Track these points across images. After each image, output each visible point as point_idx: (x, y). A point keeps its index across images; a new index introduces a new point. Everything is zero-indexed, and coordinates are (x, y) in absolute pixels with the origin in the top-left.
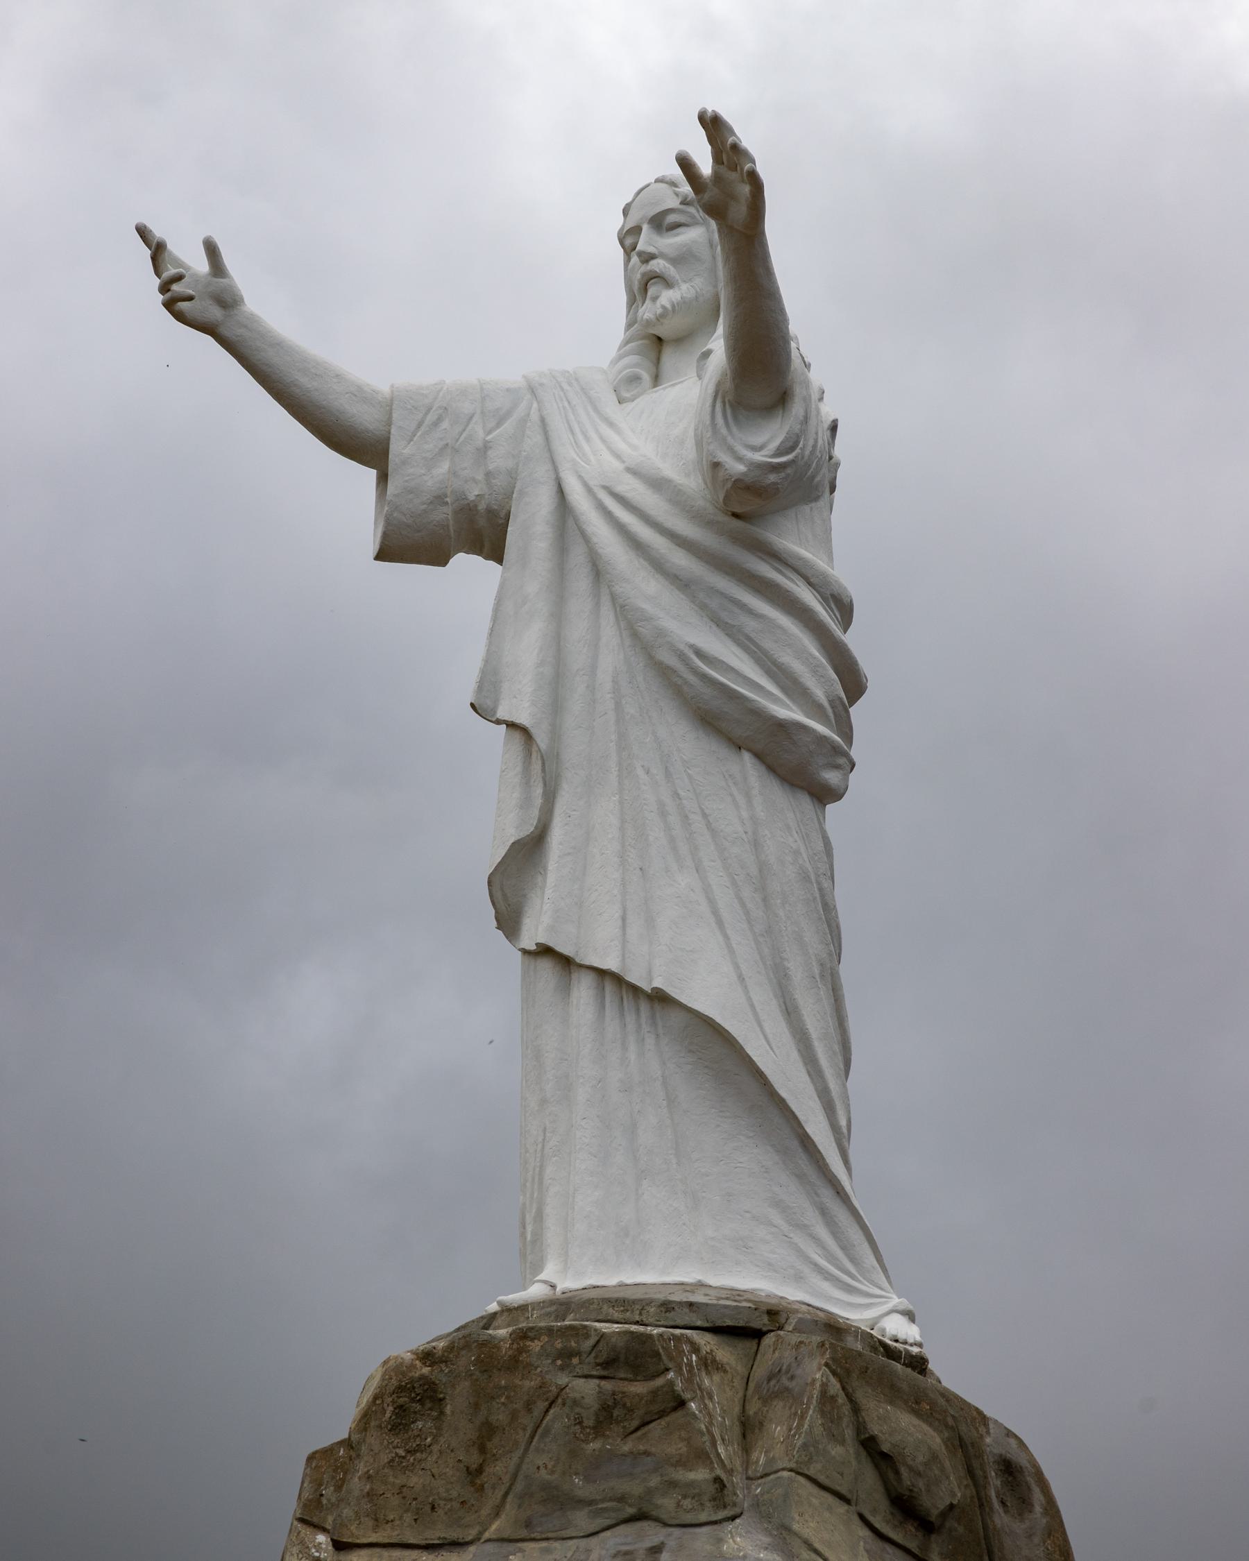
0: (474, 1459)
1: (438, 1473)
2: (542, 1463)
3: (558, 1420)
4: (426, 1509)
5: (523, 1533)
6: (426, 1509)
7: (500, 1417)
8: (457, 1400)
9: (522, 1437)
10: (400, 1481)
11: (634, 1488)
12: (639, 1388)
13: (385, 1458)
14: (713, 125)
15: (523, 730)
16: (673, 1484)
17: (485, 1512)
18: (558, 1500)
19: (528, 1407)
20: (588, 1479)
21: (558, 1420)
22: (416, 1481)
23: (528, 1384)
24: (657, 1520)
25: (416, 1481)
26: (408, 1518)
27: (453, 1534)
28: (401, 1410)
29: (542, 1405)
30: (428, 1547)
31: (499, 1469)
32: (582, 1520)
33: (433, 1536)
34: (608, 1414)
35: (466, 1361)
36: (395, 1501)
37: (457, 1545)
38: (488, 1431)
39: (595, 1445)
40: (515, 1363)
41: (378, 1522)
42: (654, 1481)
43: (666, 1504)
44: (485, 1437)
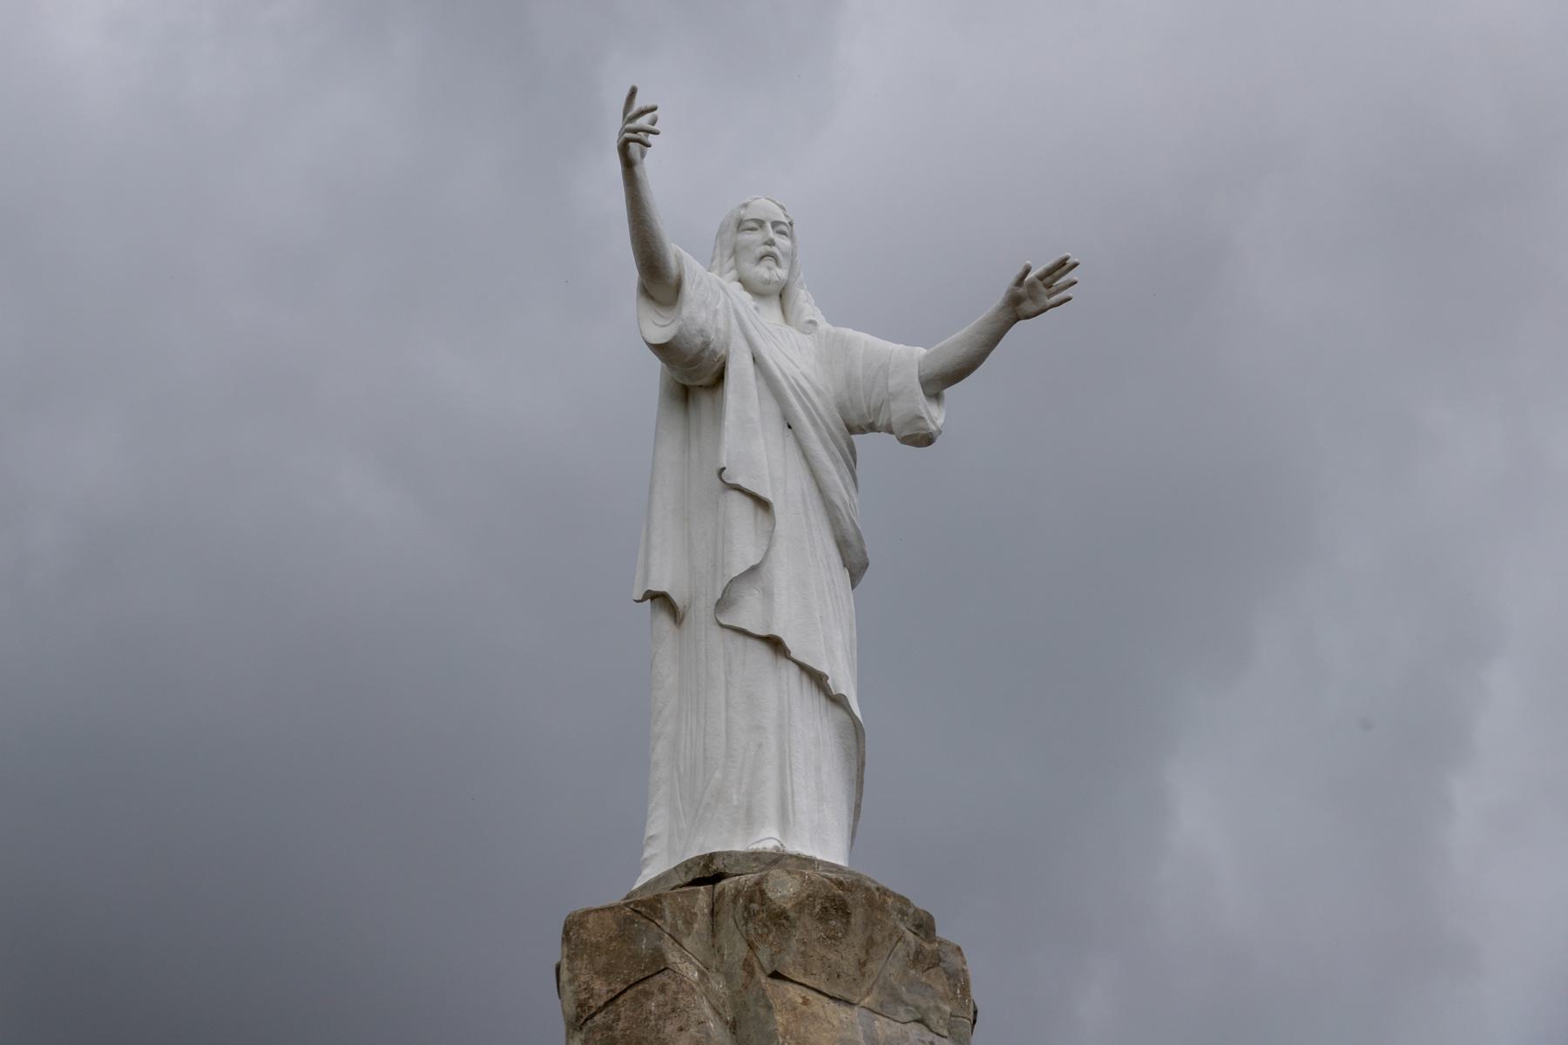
0: (863, 956)
1: (846, 957)
3: (900, 949)
4: (835, 975)
5: (878, 1009)
6: (835, 975)
7: (878, 938)
8: (857, 919)
9: (886, 953)
10: (823, 952)
11: (923, 1004)
12: (927, 946)
13: (815, 935)
14: (1076, 265)
15: (762, 504)
16: (938, 1009)
17: (864, 989)
19: (891, 935)
20: (908, 991)
21: (900, 949)
22: (833, 957)
23: (891, 924)
24: (927, 1026)
25: (833, 957)
26: (824, 976)
27: (847, 996)
28: (825, 909)
29: (895, 939)
30: (831, 998)
31: (871, 966)
32: (902, 1014)
33: (836, 992)
35: (861, 895)
36: (818, 963)
37: (848, 1003)
39: (913, 972)
40: (882, 908)
41: (806, 972)
42: (932, 1004)
43: (933, 1018)
44: (870, 943)
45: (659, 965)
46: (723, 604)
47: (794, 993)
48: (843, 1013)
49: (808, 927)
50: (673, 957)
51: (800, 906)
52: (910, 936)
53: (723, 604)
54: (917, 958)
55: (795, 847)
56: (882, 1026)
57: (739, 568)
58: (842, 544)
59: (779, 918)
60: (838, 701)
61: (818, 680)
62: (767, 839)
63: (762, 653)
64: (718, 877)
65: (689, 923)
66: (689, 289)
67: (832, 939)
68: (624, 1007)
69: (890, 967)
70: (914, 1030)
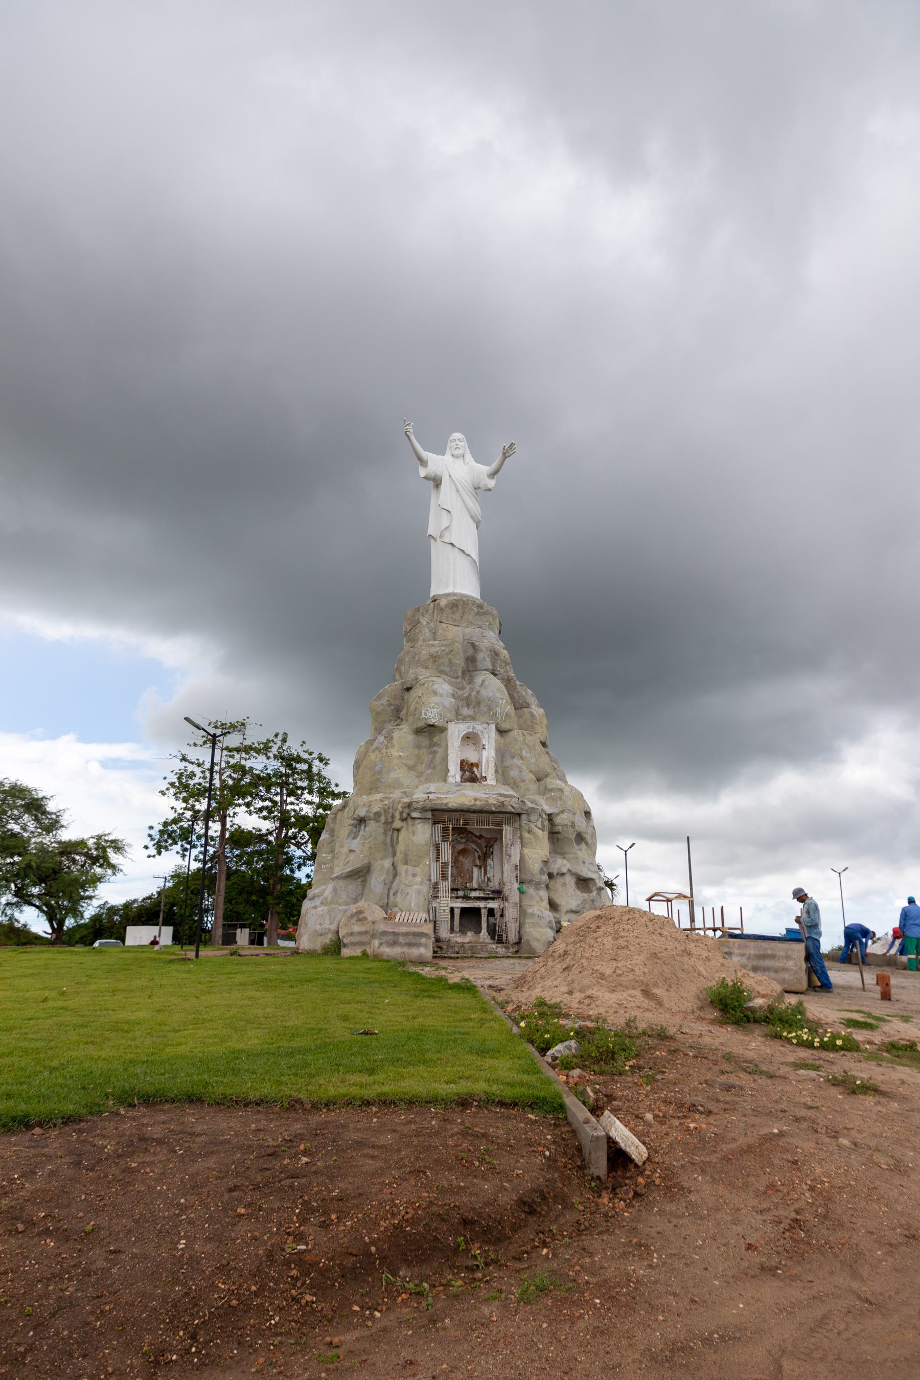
1: (457, 616)
2: (470, 617)
3: (472, 613)
8: (460, 607)
15: (449, 511)
18: (472, 623)
21: (472, 613)
34: (478, 614)
38: (464, 612)
44: (464, 612)
45: (418, 622)
46: (441, 537)
47: (444, 625)
48: (456, 628)
49: (448, 611)
50: (421, 620)
51: (446, 606)
52: (476, 609)
53: (441, 537)
54: (478, 614)
55: (456, 591)
56: (467, 630)
57: (443, 528)
58: (472, 517)
59: (442, 610)
60: (468, 555)
61: (463, 551)
62: (450, 590)
63: (450, 546)
64: (435, 600)
65: (427, 612)
66: (429, 463)
67: (454, 612)
68: (412, 631)
69: (470, 617)
70: (478, 630)
